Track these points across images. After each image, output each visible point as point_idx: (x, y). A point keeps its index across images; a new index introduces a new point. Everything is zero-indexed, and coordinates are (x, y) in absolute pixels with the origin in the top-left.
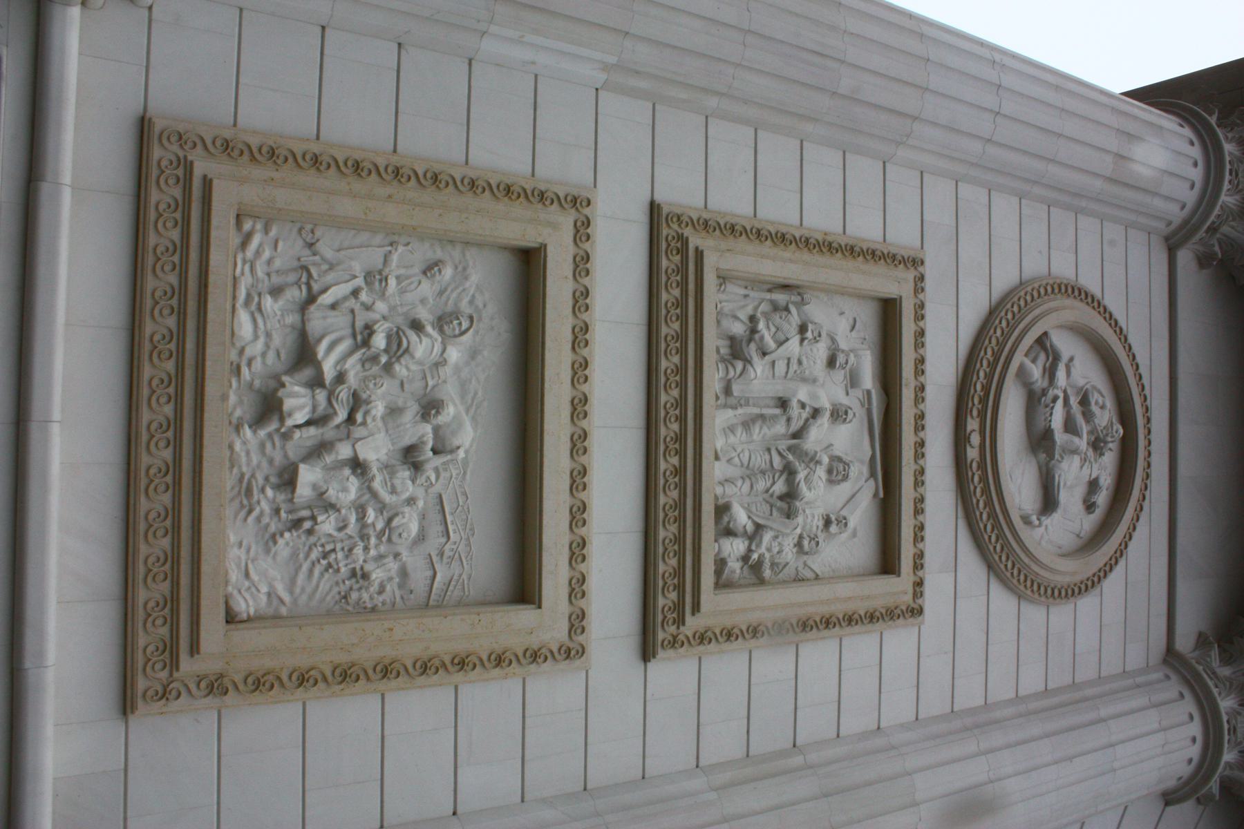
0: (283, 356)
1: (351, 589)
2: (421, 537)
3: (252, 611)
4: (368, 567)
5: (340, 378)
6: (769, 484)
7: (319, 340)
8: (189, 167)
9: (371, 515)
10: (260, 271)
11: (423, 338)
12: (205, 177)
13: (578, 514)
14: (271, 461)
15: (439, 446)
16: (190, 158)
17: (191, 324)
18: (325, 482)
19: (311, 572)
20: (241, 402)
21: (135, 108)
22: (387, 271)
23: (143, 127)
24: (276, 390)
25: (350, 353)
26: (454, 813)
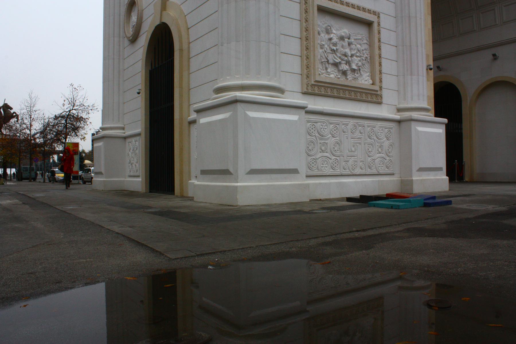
0: (335, 69)
1: (367, 61)
2: (360, 45)
3: (371, 80)
4: (365, 57)
5: (340, 58)
7: (335, 61)
8: (313, 85)
9: (358, 55)
10: (324, 72)
11: (333, 38)
12: (314, 82)
14: (350, 73)
16: (311, 85)
17: (336, 86)
19: (365, 68)
21: (301, 94)
22: (320, 44)
23: (304, 93)
24: (343, 71)
25: (336, 54)
26: (396, 47)
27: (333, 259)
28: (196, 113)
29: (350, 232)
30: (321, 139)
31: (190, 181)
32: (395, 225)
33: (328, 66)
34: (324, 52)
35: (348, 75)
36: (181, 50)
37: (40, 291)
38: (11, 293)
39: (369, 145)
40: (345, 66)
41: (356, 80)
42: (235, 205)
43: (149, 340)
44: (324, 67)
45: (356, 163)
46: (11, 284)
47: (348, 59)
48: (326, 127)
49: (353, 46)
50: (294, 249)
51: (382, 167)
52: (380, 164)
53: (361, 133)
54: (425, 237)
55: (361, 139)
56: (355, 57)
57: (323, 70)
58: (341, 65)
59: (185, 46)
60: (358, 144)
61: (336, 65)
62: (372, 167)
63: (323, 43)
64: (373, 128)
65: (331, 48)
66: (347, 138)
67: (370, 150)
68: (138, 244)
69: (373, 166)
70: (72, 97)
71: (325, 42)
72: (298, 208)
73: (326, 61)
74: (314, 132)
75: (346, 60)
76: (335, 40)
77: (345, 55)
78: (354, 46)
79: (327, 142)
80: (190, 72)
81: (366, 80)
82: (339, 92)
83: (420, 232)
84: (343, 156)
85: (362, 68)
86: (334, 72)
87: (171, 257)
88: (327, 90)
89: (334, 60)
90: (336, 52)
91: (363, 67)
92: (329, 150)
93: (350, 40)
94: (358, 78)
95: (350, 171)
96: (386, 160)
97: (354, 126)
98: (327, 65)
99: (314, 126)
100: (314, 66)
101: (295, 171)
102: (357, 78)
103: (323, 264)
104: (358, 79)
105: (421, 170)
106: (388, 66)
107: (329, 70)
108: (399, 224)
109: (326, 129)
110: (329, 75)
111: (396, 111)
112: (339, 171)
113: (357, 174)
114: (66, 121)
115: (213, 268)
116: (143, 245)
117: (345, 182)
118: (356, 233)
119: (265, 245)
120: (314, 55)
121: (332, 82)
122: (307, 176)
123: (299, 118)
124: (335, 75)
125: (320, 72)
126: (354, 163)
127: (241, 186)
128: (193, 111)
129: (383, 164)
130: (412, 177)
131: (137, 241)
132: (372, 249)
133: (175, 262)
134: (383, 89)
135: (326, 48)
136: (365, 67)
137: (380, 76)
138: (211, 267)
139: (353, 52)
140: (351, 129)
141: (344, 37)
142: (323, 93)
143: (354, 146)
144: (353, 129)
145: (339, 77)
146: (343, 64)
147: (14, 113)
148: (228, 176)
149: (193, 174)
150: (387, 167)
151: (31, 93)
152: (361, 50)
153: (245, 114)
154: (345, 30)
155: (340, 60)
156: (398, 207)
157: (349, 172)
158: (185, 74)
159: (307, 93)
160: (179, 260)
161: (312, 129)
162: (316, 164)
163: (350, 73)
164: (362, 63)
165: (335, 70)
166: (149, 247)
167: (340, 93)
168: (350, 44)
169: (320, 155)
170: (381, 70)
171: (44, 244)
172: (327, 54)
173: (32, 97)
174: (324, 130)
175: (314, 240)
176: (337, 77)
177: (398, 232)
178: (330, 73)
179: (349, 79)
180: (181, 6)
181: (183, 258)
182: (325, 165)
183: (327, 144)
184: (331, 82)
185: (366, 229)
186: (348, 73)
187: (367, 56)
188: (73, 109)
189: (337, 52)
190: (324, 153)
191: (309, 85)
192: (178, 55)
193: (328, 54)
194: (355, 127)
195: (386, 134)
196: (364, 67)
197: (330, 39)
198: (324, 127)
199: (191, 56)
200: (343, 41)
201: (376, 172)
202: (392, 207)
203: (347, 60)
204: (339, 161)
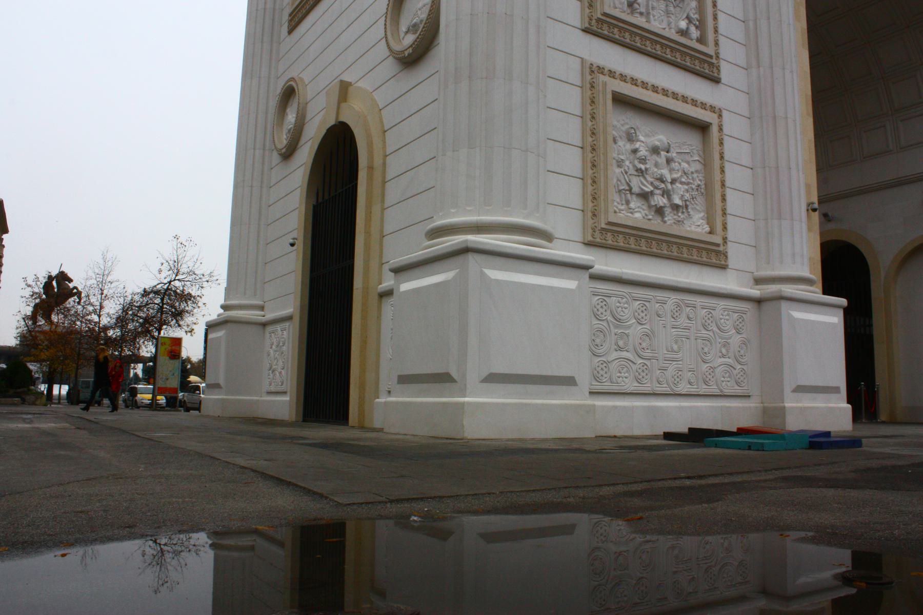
0: (643, 203)
1: (700, 191)
2: (688, 163)
4: (696, 184)
5: (652, 184)
6: (672, 5)
8: (603, 229)
9: (683, 180)
10: (623, 207)
12: (606, 224)
13: (675, 96)
14: (671, 212)
15: (667, 150)
16: (599, 229)
18: (678, 194)
19: (696, 204)
20: (656, 220)
22: (617, 158)
23: (589, 244)
25: (645, 178)
26: (752, 169)
27: (647, 514)
28: (393, 274)
29: (675, 479)
30: (616, 327)
31: (377, 400)
32: (759, 471)
33: (631, 197)
34: (624, 172)
35: (666, 215)
36: (371, 168)
37: (93, 536)
38: (39, 536)
39: (704, 342)
40: (661, 199)
41: (681, 224)
42: (459, 437)
43: (295, 610)
44: (624, 199)
45: (680, 373)
46: (41, 525)
47: (666, 186)
48: (626, 305)
49: (675, 165)
50: (571, 500)
51: (728, 381)
52: (724, 377)
53: (689, 319)
54: (819, 487)
55: (689, 329)
56: (678, 185)
57: (622, 204)
58: (653, 196)
59: (378, 161)
60: (684, 339)
61: (645, 196)
62: (710, 382)
63: (622, 157)
64: (711, 311)
65: (637, 167)
66: (664, 327)
67: (706, 350)
68: (280, 481)
69: (712, 379)
70: (176, 259)
71: (626, 155)
72: (575, 445)
73: (627, 188)
74: (604, 313)
75: (663, 188)
76: (643, 152)
77: (661, 180)
78: (677, 164)
79: (627, 332)
80: (386, 207)
81: (699, 226)
82: (651, 244)
83: (810, 482)
84: (657, 360)
85: (691, 203)
86: (641, 208)
87: (340, 502)
88: (629, 240)
89: (640, 187)
90: (644, 173)
91: (693, 202)
92: (631, 347)
93: (669, 155)
94: (684, 222)
95: (670, 387)
96: (735, 369)
97: (676, 306)
98: (629, 196)
99: (604, 303)
100: (605, 196)
101: (570, 381)
102: (683, 222)
103: (628, 520)
104: (684, 224)
105: (800, 389)
106: (736, 203)
107: (632, 205)
108: (766, 471)
109: (626, 308)
110: (632, 213)
111: (752, 281)
112: (650, 386)
113: (683, 393)
114: (162, 299)
115: (420, 519)
116: (289, 484)
117: (661, 407)
118: (687, 480)
119: (517, 492)
120: (606, 177)
121: (638, 226)
122: (591, 393)
123: (579, 287)
124: (642, 215)
125: (617, 207)
126: (678, 373)
127: (469, 403)
128: (388, 270)
129: (730, 377)
130: (783, 403)
131: (277, 479)
132: (720, 502)
133: (349, 509)
134: (729, 243)
135: (628, 166)
136: (697, 202)
137: (724, 218)
138: (415, 518)
139: (675, 176)
140: (672, 311)
141: (659, 148)
142: (622, 244)
143: (676, 342)
144: (675, 311)
145: (650, 217)
146: (657, 194)
147: (75, 288)
148: (448, 384)
149: (383, 387)
150: (738, 383)
151: (105, 251)
152: (689, 172)
153: (483, 274)
154: (661, 137)
155: (652, 189)
156: (761, 447)
157: (669, 389)
158: (376, 209)
159: (591, 243)
160: (355, 507)
161: (602, 307)
162: (607, 372)
163: (671, 212)
164: (692, 195)
165: (643, 205)
166: (301, 487)
167: (652, 247)
168: (669, 161)
169: (615, 355)
170: (725, 209)
171: (108, 477)
172: (628, 177)
173: (108, 259)
174: (622, 311)
175: (608, 488)
176: (646, 217)
177: (766, 481)
178: (634, 209)
179: (669, 222)
180: (373, 93)
181: (364, 503)
182: (625, 373)
183: (628, 335)
184: (635, 225)
185: (704, 476)
186: (667, 212)
187: (699, 183)
188: (175, 280)
189: (647, 174)
190: (622, 352)
191: (596, 230)
192: (365, 176)
193: (630, 177)
194: (679, 308)
195: (735, 322)
196: (695, 203)
197: (635, 151)
198: (622, 304)
199: (388, 177)
200: (658, 156)
201: (717, 392)
202: (750, 446)
203: (665, 188)
204: (649, 366)
